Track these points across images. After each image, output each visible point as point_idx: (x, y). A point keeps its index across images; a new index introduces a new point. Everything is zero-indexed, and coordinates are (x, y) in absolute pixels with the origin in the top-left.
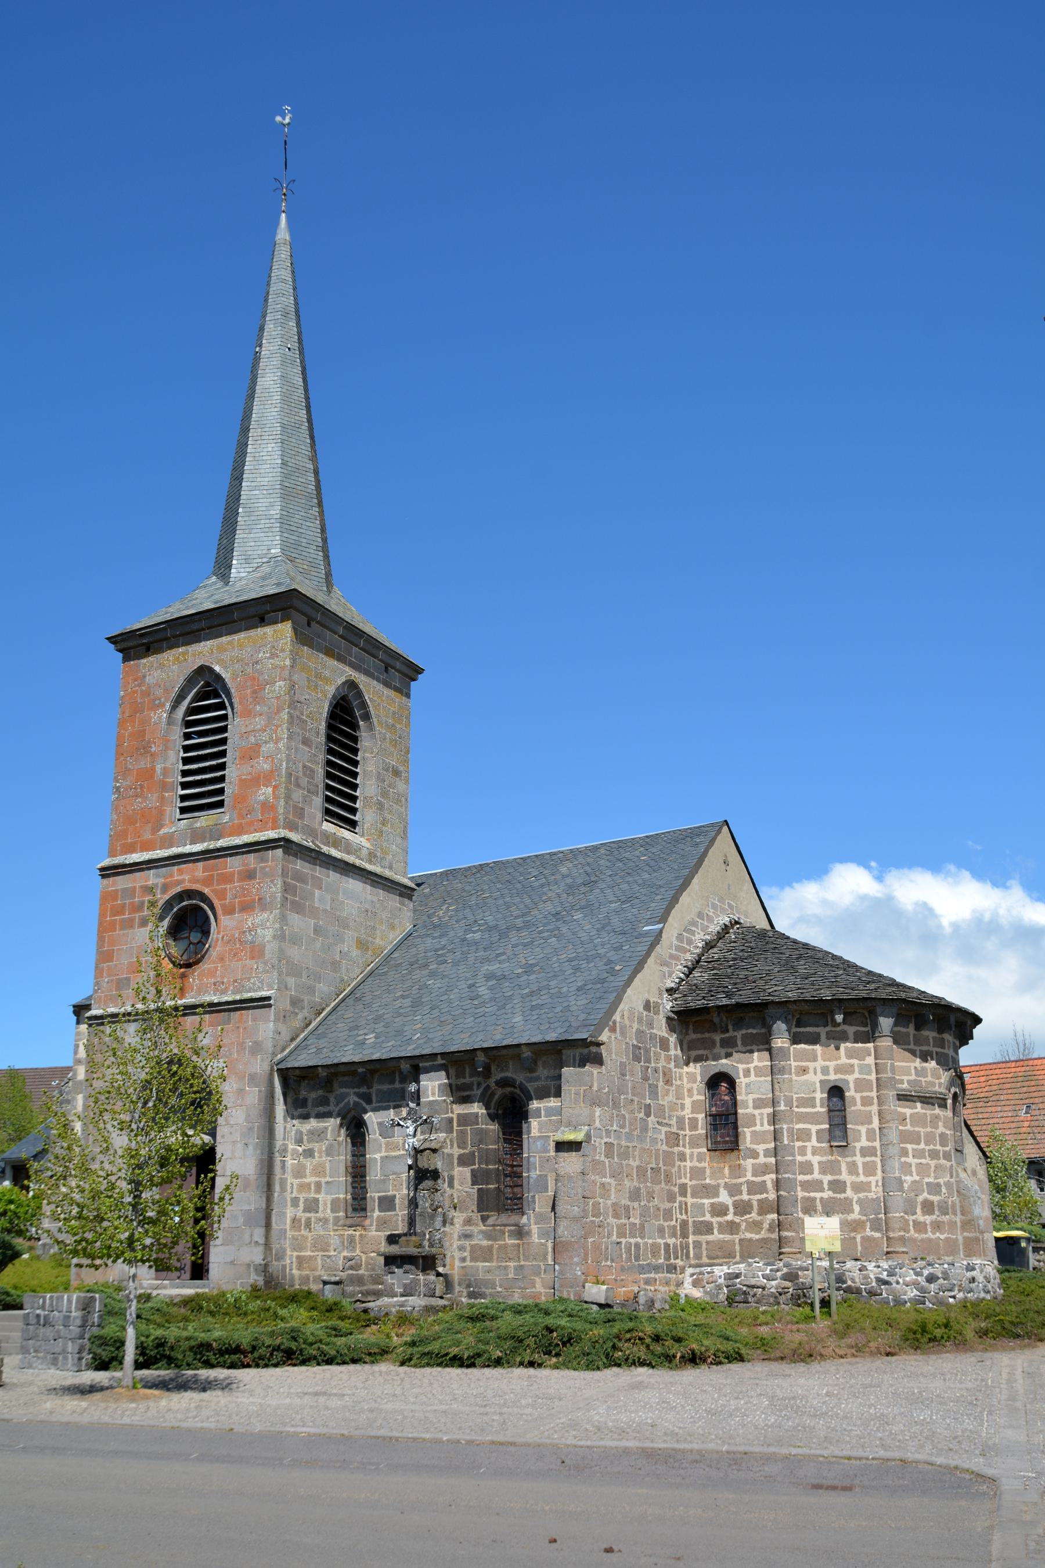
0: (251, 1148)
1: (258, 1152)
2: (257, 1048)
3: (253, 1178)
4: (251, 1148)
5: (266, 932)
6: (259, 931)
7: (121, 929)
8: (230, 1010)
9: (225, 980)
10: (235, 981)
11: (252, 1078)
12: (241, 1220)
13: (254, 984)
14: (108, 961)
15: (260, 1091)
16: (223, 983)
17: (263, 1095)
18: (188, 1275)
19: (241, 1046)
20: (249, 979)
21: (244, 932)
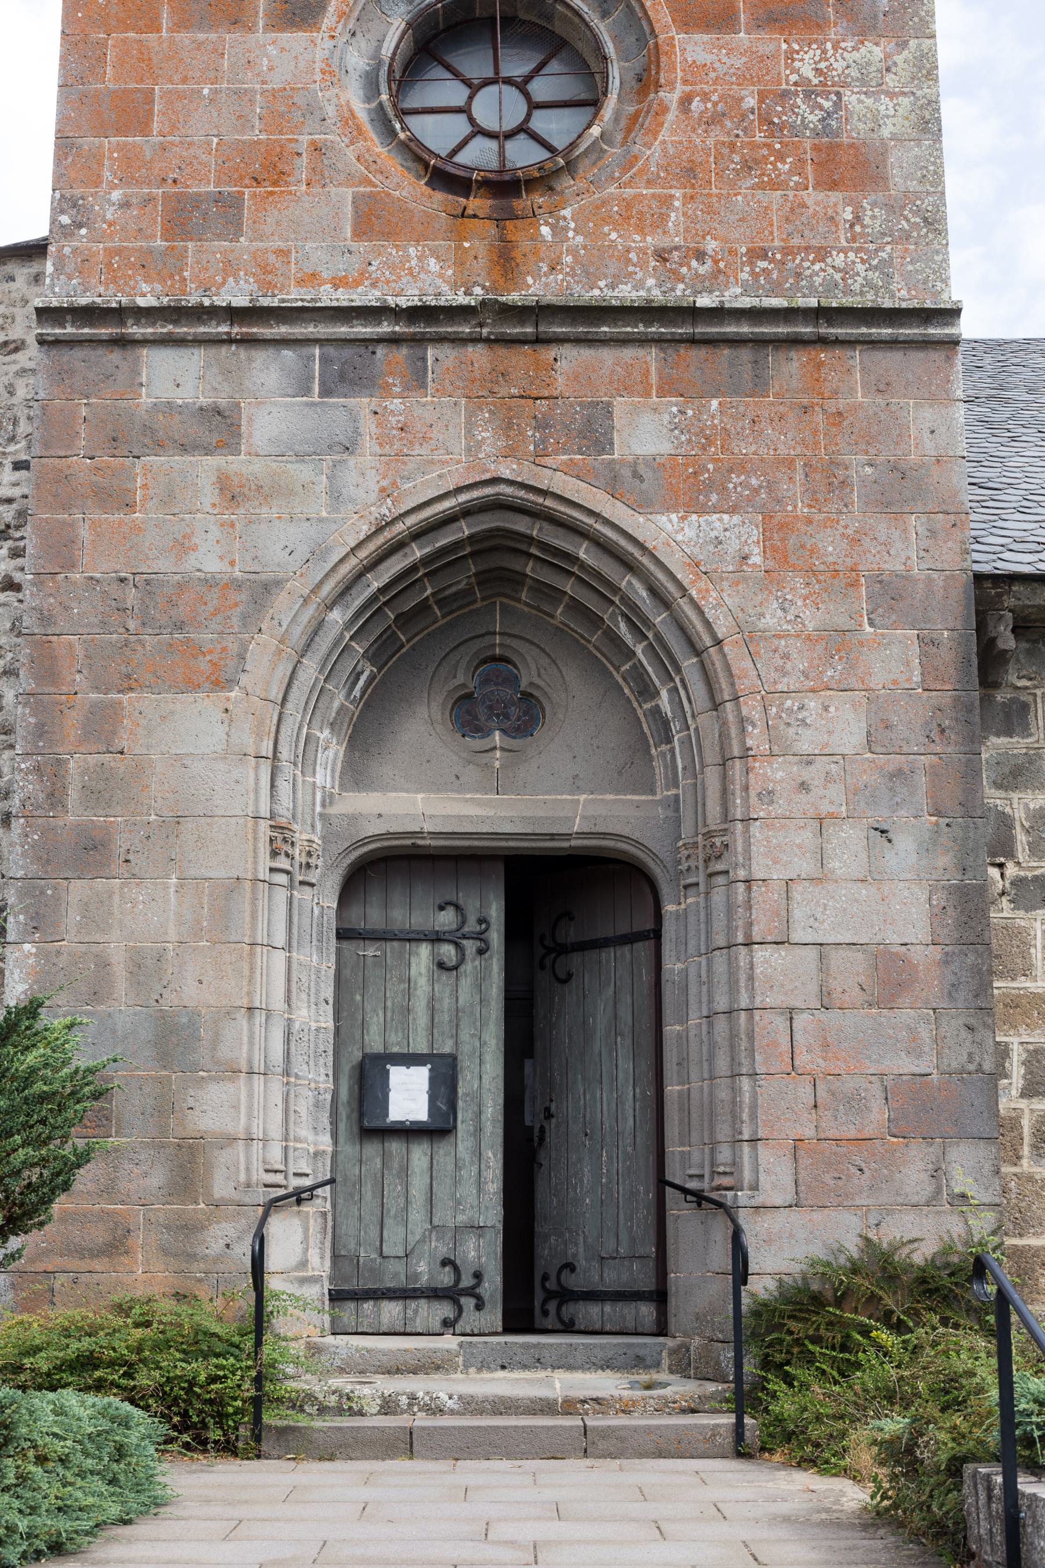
0: (905, 844)
1: (945, 860)
2: (901, 488)
3: (924, 956)
4: (905, 844)
5: (885, 104)
6: (850, 98)
7: (181, 25)
8: (760, 342)
9: (711, 245)
10: (758, 253)
11: (890, 595)
12: (877, 1115)
13: (846, 271)
14: (121, 130)
15: (927, 642)
16: (701, 255)
17: (947, 656)
18: (494, 1317)
19: (829, 481)
20: (822, 254)
21: (785, 95)
